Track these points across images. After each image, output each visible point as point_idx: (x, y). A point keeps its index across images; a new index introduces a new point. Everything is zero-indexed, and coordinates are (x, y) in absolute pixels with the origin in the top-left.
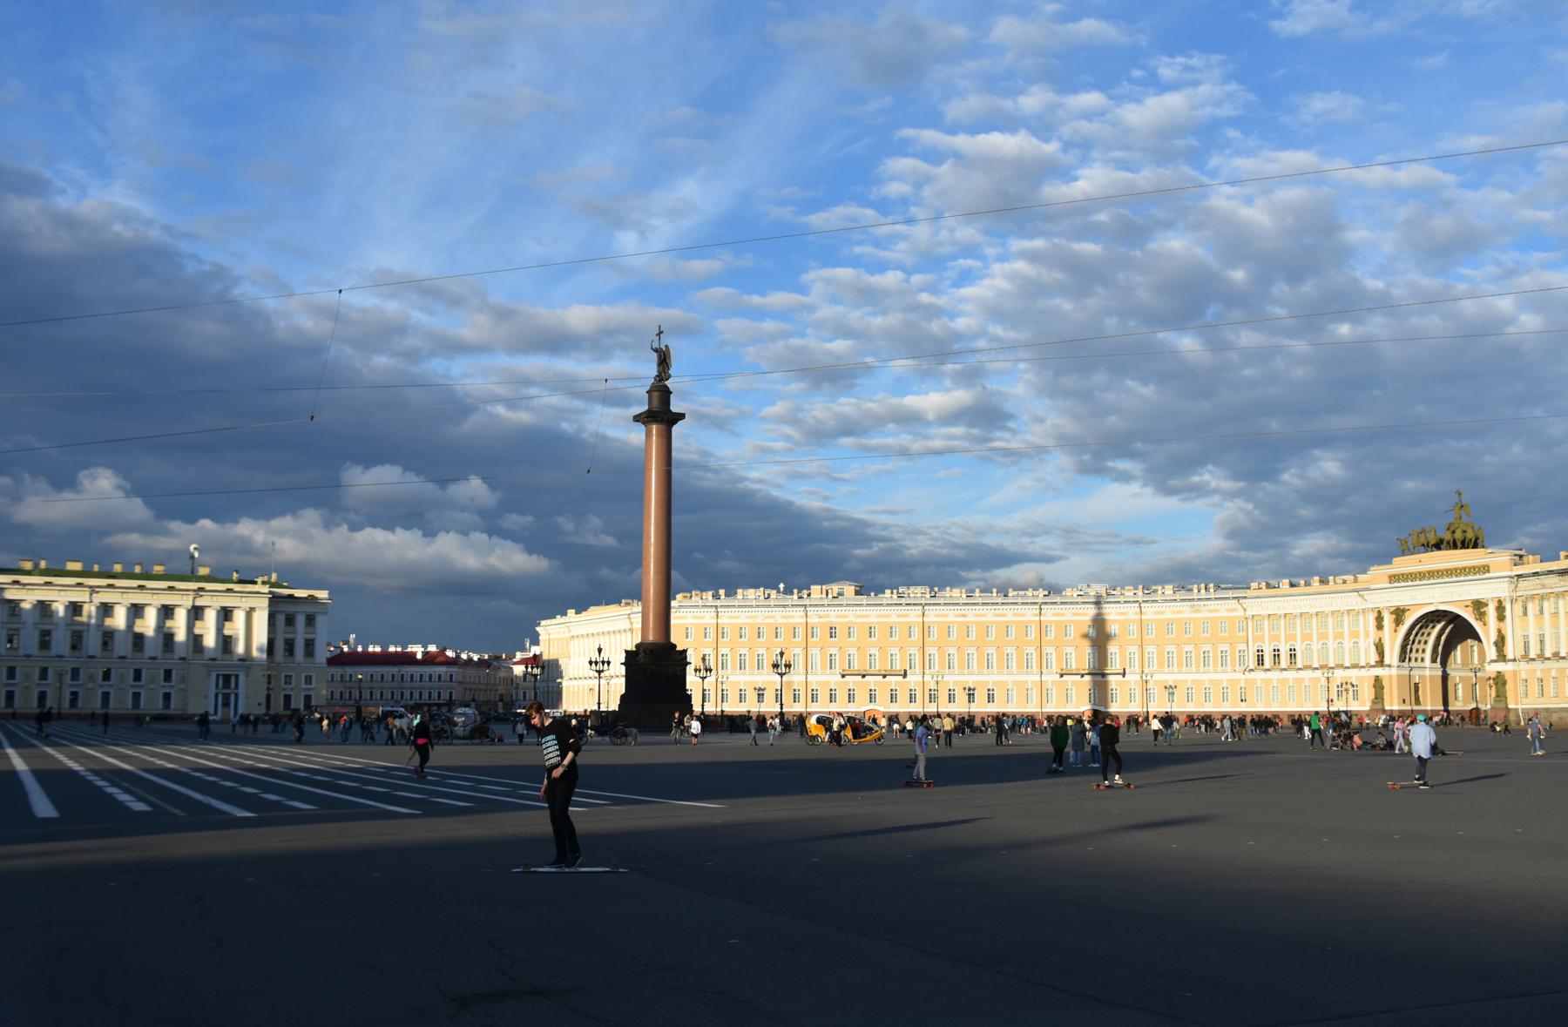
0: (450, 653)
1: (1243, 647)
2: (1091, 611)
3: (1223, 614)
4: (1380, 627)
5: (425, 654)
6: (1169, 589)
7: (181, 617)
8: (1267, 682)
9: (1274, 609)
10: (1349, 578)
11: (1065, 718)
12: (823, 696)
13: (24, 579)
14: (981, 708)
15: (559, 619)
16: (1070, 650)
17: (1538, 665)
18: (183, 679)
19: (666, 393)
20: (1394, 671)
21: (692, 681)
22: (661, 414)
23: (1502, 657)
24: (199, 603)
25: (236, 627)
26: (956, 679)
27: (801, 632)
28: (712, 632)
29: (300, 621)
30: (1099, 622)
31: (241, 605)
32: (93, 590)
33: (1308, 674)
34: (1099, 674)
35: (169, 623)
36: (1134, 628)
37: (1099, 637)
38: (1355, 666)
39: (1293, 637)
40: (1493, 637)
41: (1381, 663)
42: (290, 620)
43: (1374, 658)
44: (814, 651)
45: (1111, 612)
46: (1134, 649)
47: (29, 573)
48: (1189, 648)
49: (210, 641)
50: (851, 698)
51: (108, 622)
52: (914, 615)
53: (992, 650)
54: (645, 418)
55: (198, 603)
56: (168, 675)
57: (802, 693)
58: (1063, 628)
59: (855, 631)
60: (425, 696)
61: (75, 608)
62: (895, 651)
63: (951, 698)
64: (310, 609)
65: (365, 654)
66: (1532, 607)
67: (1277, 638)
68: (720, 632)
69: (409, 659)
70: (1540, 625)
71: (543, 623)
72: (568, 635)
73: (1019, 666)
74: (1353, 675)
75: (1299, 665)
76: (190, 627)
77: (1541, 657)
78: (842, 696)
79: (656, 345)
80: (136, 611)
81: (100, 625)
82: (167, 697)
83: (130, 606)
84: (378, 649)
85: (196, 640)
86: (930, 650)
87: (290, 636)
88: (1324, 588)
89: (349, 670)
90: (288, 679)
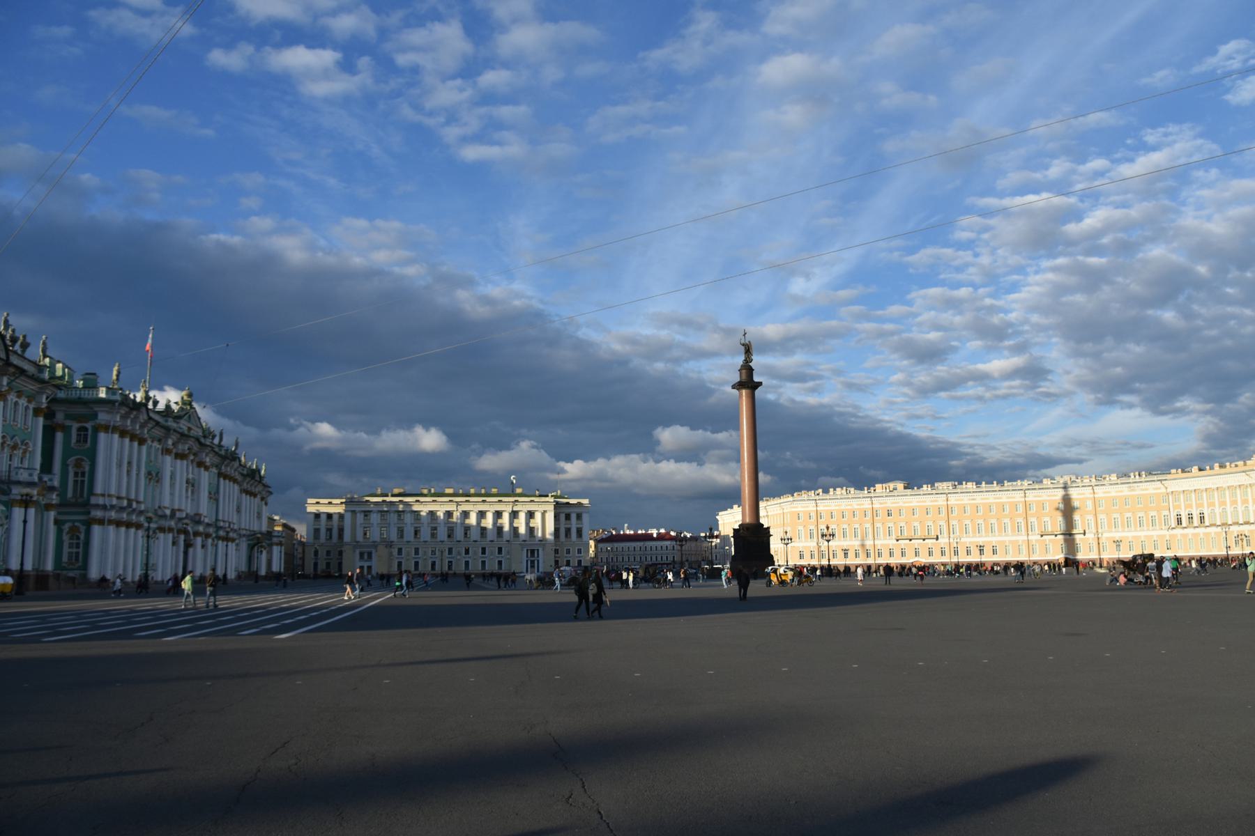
0: (673, 533)
1: (1166, 513)
2: (1061, 493)
5: (659, 534)
6: (1114, 477)
7: (506, 517)
8: (1184, 536)
10: (1240, 463)
11: (803, 567)
12: (885, 553)
13: (422, 499)
14: (988, 558)
16: (1046, 519)
18: (508, 553)
21: (775, 546)
22: (748, 383)
25: (537, 522)
26: (971, 540)
27: (869, 514)
28: (813, 515)
29: (574, 517)
30: (1067, 500)
32: (458, 503)
33: (1213, 529)
34: (1069, 535)
36: (1090, 504)
37: (1068, 510)
38: (1247, 523)
39: (1202, 505)
42: (568, 517)
44: (878, 525)
45: (1074, 493)
46: (1091, 517)
47: (425, 496)
48: (1129, 515)
49: (522, 530)
50: (903, 554)
51: (467, 521)
52: (941, 500)
53: (994, 521)
54: (739, 386)
56: (500, 550)
58: (1042, 505)
59: (903, 512)
61: (449, 514)
62: (930, 523)
63: (968, 552)
64: (578, 510)
65: (625, 535)
67: (1190, 506)
69: (649, 537)
73: (1013, 530)
75: (1207, 523)
76: (511, 523)
78: (897, 553)
80: (482, 515)
81: (463, 523)
82: (500, 563)
83: (481, 512)
85: (515, 530)
86: (953, 522)
88: (1223, 471)
89: (616, 545)
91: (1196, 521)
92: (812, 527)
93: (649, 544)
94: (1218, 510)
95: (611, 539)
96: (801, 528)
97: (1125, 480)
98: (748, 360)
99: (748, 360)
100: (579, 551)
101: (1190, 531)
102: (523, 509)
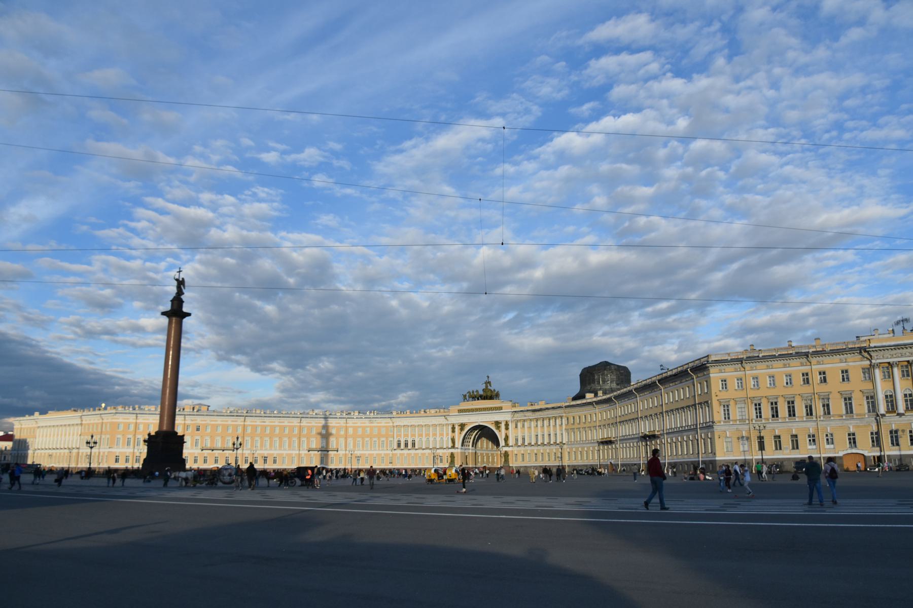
2: (323, 422)
3: (383, 424)
4: (453, 431)
6: (357, 413)
8: (402, 455)
9: (408, 425)
17: (522, 448)
19: (181, 302)
20: (459, 451)
23: (507, 445)
30: (326, 427)
37: (325, 435)
39: (414, 435)
40: (503, 437)
41: (453, 447)
43: (450, 445)
45: (332, 423)
46: (342, 441)
50: (205, 461)
58: (310, 429)
66: (520, 425)
70: (555, 430)
74: (440, 452)
77: (543, 444)
79: (177, 277)
91: (410, 446)
94: (424, 439)
97: (402, 415)
98: (180, 292)
99: (180, 292)
101: (406, 452)
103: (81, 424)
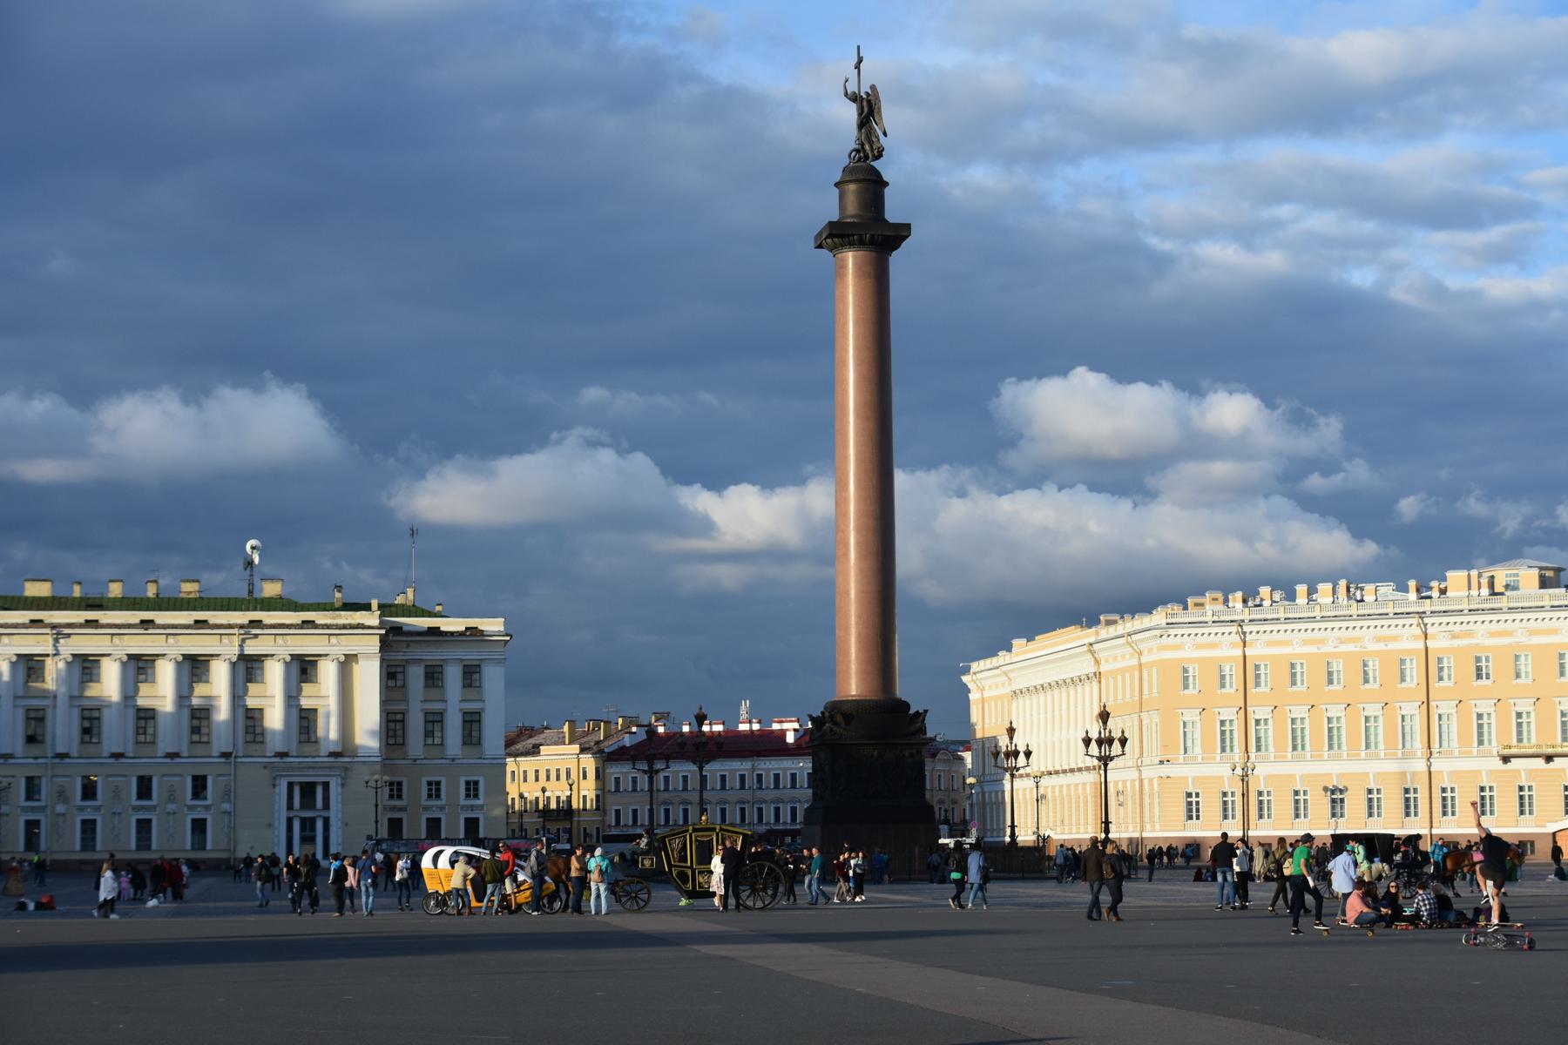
15: (1003, 657)
18: (227, 794)
24: (252, 648)
25: (323, 692)
28: (1233, 672)
29: (453, 676)
31: (327, 648)
32: (59, 631)
35: (200, 690)
42: (434, 676)
44: (1443, 707)
49: (275, 719)
51: (93, 691)
54: (837, 236)
55: (248, 651)
56: (199, 784)
57: (1422, 797)
59: (1526, 666)
60: (769, 815)
64: (470, 654)
68: (1249, 672)
71: (975, 666)
72: (1007, 690)
76: (237, 696)
78: (1505, 801)
79: (852, 88)
82: (199, 826)
84: (718, 728)
85: (251, 719)
87: (437, 706)
90: (434, 790)
92: (1229, 713)
93: (770, 766)
95: (652, 750)
96: (1191, 715)
100: (472, 789)
102: (277, 649)
103: (1098, 675)
